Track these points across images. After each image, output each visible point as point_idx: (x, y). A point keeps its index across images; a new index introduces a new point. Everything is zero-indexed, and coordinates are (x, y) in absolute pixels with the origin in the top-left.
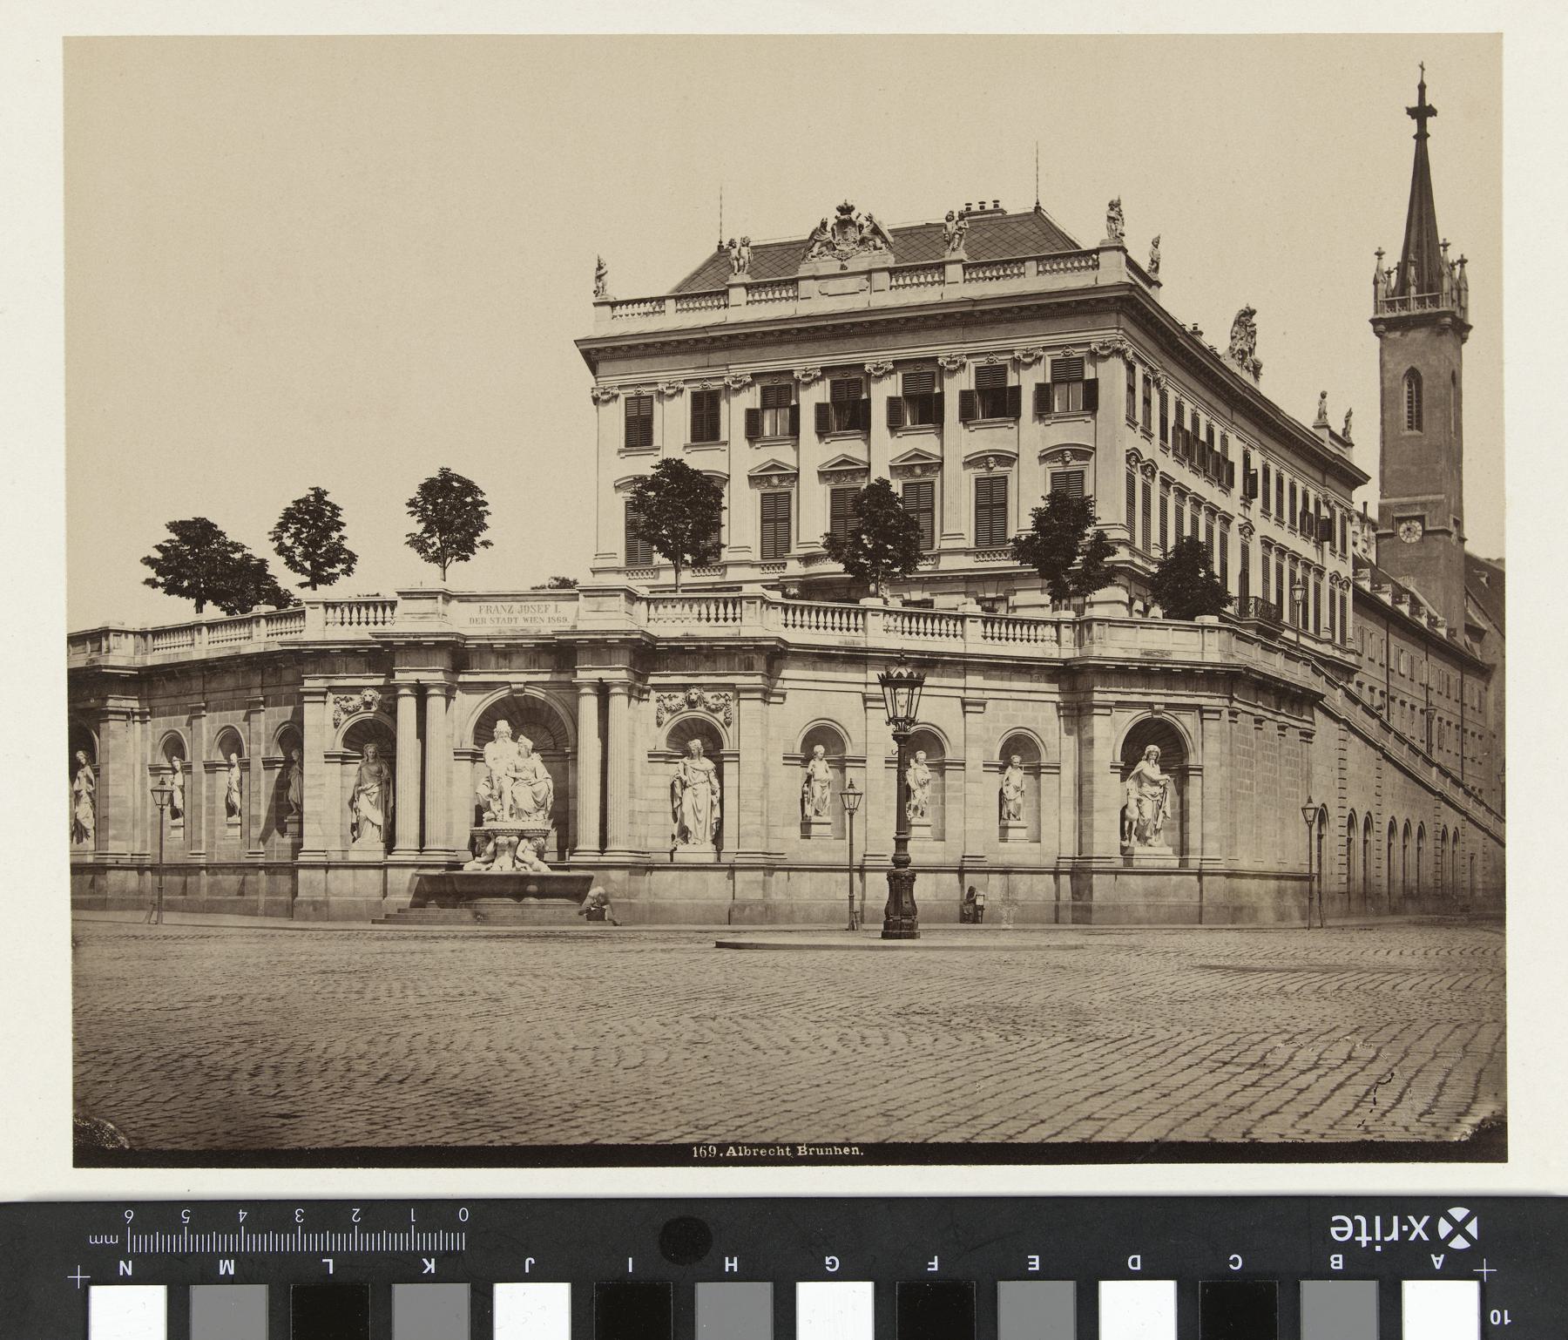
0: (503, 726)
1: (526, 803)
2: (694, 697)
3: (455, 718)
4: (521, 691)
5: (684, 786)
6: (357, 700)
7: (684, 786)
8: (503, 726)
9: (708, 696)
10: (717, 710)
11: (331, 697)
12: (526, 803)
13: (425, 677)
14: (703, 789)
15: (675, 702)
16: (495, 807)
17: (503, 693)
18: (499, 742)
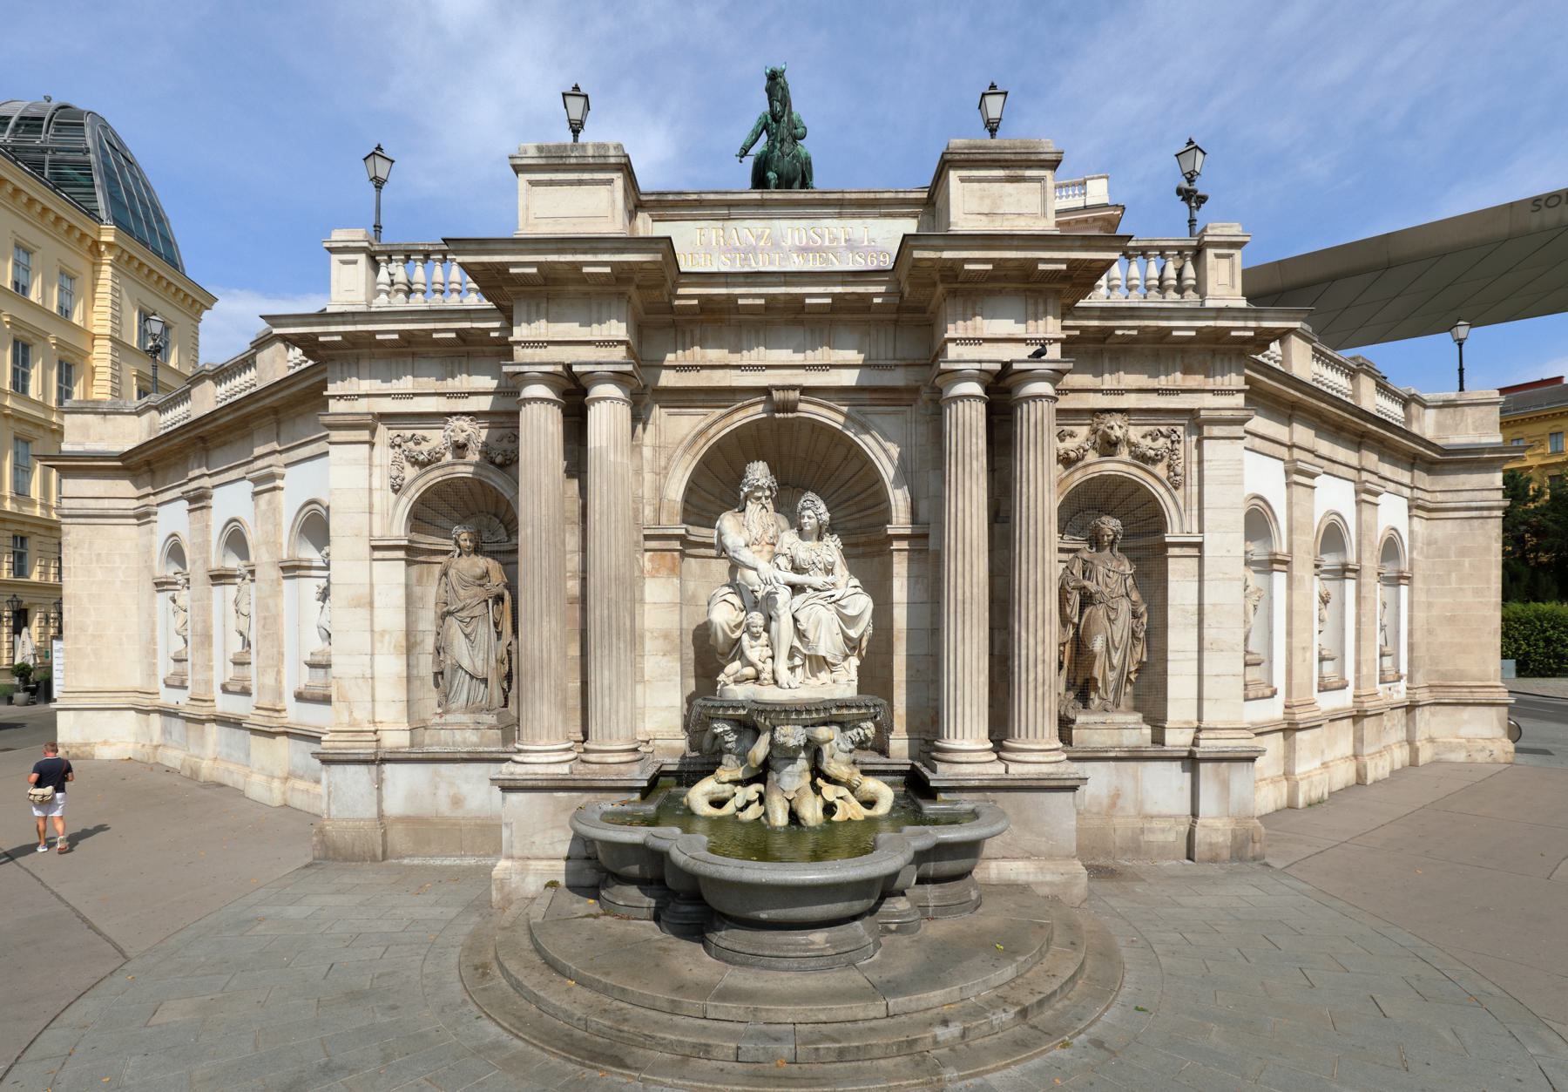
0: (759, 473)
1: (827, 642)
2: (1118, 433)
3: (645, 459)
4: (791, 407)
5: (1087, 600)
6: (436, 438)
7: (1087, 600)
8: (759, 473)
9: (1135, 434)
10: (1154, 461)
11: (384, 434)
12: (827, 642)
14: (1124, 607)
15: (1070, 444)
16: (755, 651)
17: (756, 412)
18: (752, 507)
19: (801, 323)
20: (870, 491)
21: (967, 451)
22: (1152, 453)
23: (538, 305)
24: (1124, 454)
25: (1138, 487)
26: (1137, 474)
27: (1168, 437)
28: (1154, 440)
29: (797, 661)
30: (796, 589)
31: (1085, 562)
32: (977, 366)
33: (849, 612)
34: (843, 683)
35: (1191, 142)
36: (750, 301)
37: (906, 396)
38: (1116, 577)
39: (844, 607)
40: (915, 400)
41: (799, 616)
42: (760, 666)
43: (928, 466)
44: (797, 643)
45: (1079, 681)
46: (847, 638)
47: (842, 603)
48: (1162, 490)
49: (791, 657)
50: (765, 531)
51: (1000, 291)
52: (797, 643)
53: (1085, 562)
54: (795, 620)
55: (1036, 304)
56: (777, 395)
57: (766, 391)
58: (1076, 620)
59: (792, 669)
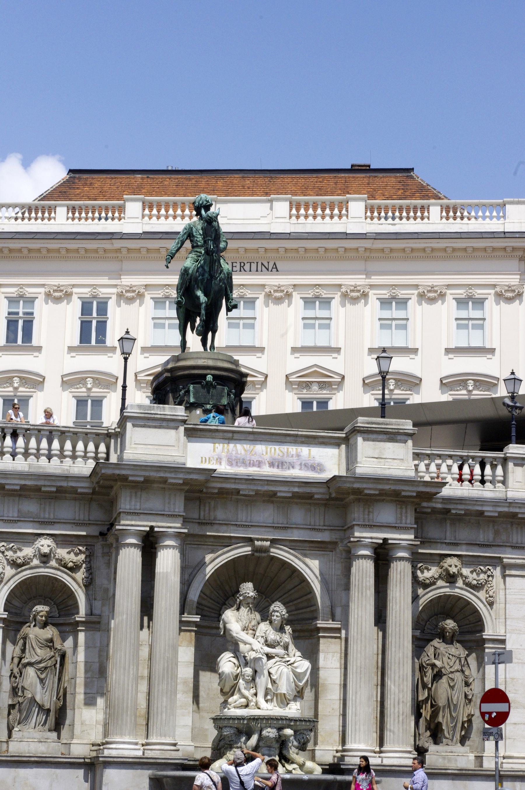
0: (248, 589)
2: (453, 570)
4: (266, 550)
8: (248, 589)
13: (161, 525)
19: (272, 502)
20: (305, 598)
21: (364, 585)
22: (475, 582)
23: (136, 493)
24: (460, 583)
25: (468, 603)
26: (467, 595)
27: (485, 573)
28: (478, 574)
29: (269, 697)
30: (269, 657)
31: (436, 648)
32: (370, 540)
33: (299, 670)
34: (294, 710)
35: (513, 373)
36: (246, 493)
37: (329, 546)
38: (454, 659)
39: (296, 668)
40: (335, 549)
41: (272, 671)
42: (250, 698)
43: (340, 584)
44: (270, 686)
45: (432, 726)
46: (296, 685)
47: (295, 665)
48: (481, 605)
49: (266, 695)
50: (250, 622)
51: (383, 500)
52: (270, 686)
53: (436, 648)
54: (270, 673)
55: (401, 508)
56: (257, 543)
57: (250, 541)
58: (430, 686)
59: (267, 701)
